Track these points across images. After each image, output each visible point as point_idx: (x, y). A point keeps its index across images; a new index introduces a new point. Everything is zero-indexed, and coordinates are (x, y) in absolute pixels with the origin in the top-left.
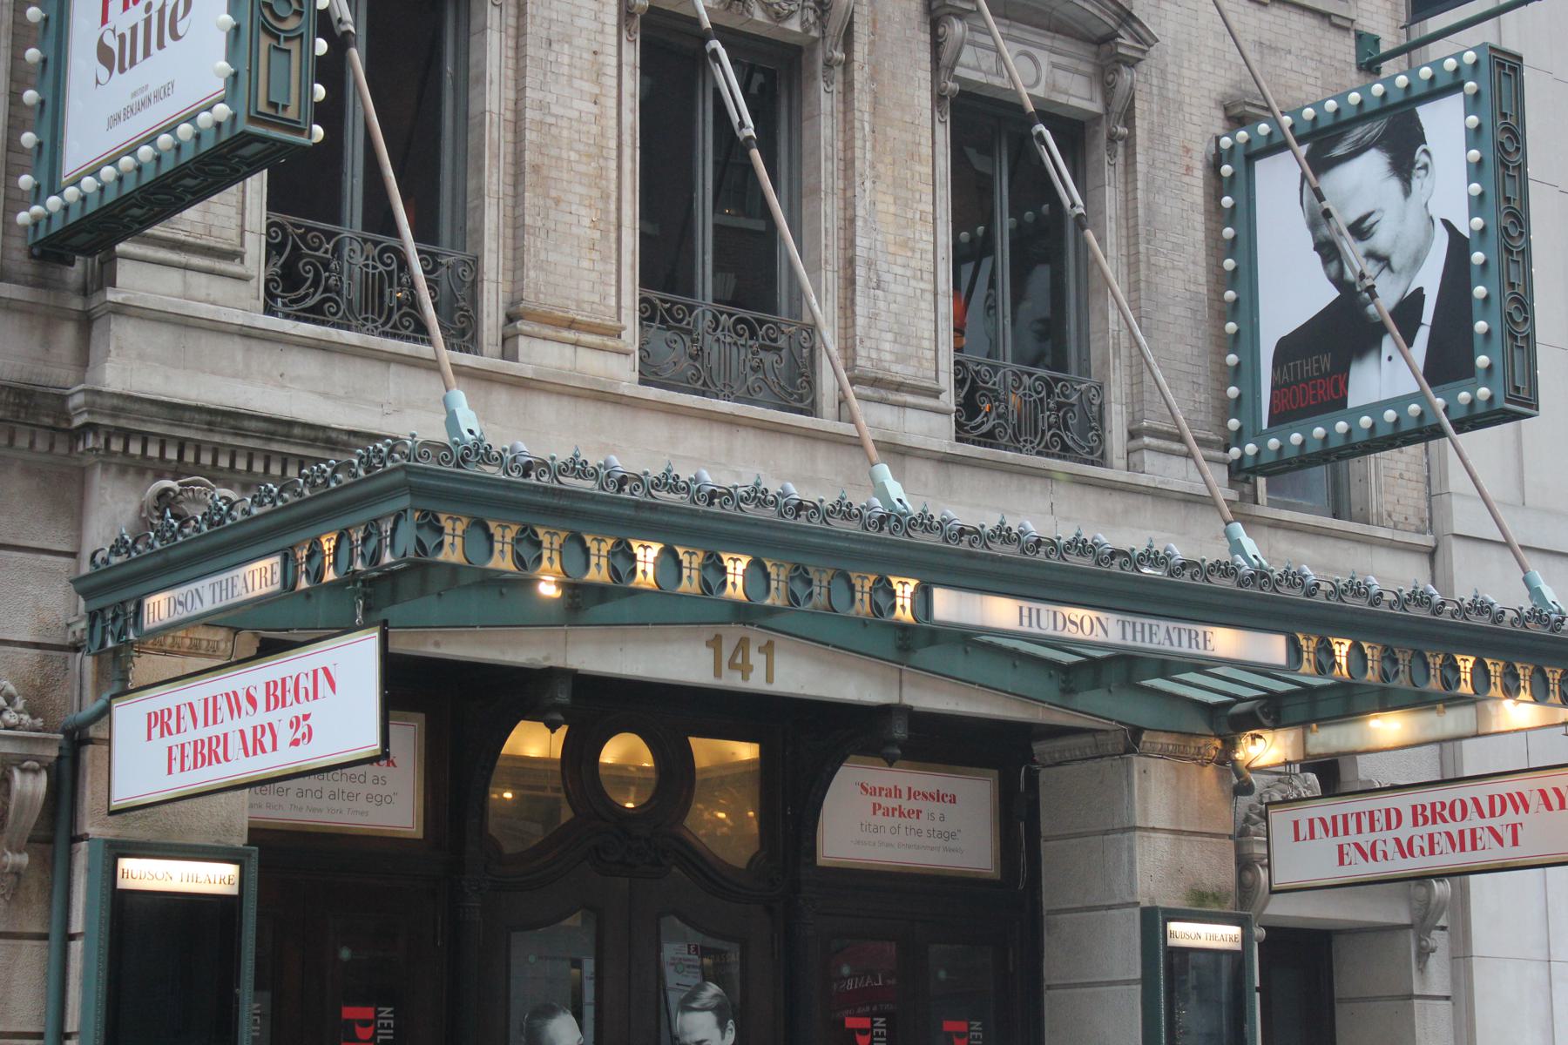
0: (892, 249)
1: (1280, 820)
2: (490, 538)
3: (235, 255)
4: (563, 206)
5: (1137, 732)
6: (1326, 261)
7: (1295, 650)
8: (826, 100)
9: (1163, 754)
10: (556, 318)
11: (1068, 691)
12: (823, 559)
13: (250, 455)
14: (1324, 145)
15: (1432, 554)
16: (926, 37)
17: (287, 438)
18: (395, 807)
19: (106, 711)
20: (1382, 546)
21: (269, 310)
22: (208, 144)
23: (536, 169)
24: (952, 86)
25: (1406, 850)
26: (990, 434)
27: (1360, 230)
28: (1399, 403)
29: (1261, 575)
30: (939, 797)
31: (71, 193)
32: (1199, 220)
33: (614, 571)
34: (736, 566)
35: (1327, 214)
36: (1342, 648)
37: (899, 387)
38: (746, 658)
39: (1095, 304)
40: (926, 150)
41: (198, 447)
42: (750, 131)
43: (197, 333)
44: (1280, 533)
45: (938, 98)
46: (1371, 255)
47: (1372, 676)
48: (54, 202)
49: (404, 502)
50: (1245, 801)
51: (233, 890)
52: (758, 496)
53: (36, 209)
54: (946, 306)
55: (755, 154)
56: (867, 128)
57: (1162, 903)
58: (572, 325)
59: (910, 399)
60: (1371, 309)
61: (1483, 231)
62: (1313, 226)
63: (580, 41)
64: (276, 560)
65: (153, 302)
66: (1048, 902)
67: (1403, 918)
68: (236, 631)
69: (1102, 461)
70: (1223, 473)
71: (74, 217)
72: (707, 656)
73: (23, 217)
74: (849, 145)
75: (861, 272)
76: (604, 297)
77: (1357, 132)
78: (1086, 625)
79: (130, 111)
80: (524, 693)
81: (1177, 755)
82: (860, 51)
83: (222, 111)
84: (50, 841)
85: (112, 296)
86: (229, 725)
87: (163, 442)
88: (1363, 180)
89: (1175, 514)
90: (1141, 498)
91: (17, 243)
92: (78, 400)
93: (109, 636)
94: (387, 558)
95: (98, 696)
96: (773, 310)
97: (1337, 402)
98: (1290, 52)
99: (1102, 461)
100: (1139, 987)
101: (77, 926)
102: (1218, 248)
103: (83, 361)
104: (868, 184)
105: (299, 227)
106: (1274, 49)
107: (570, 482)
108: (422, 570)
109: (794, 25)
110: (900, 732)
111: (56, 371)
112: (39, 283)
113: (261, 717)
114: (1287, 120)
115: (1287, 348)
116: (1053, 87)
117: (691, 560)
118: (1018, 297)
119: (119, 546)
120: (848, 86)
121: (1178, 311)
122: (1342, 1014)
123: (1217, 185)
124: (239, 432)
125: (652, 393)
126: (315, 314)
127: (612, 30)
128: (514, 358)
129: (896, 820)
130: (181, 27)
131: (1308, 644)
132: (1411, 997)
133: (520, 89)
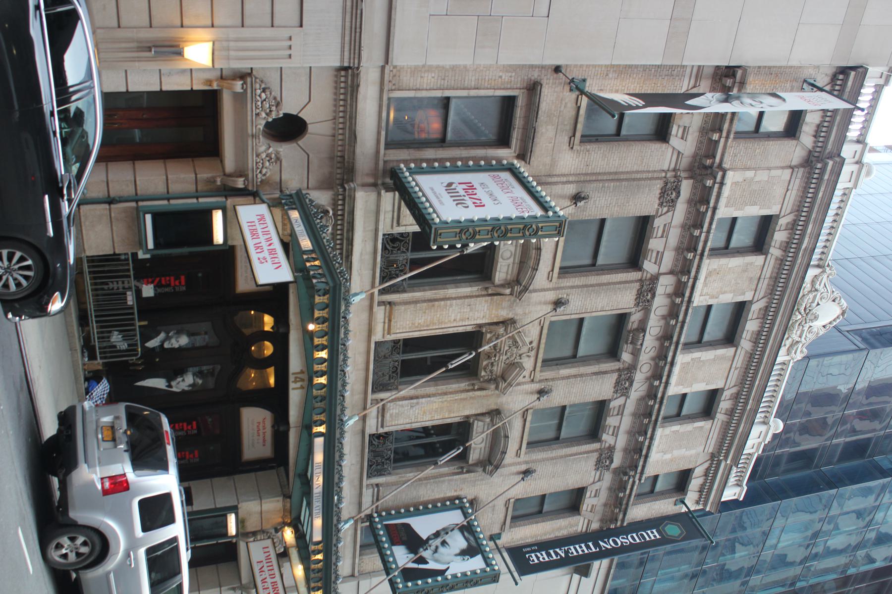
1: (268, 542)
2: (323, 309)
3: (398, 224)
5: (290, 497)
6: (434, 534)
7: (318, 543)
8: (463, 385)
9: (284, 506)
11: (300, 476)
12: (329, 405)
13: (342, 235)
14: (467, 529)
15: (353, 576)
16: (484, 411)
17: (348, 245)
18: (243, 285)
19: (263, 202)
21: (384, 235)
22: (427, 217)
23: (433, 306)
24: (471, 420)
25: (264, 581)
27: (444, 543)
28: (395, 561)
29: (339, 531)
30: (264, 441)
31: (410, 179)
32: (442, 496)
33: (318, 346)
34: (323, 380)
35: (447, 533)
36: (320, 557)
37: (383, 416)
39: (414, 469)
40: (452, 415)
41: (342, 220)
42: (450, 367)
43: (374, 217)
45: (468, 417)
46: (437, 547)
47: (313, 566)
48: (407, 174)
49: (331, 284)
50: (273, 531)
51: (215, 243)
52: (344, 385)
53: (405, 169)
54: (408, 427)
55: (444, 369)
57: (240, 511)
58: (390, 321)
59: (380, 420)
60: (421, 550)
61: (447, 579)
62: (444, 529)
63: (471, 314)
64: (311, 248)
65: (383, 203)
66: (237, 477)
67: (244, 581)
68: (291, 235)
69: (368, 477)
70: (368, 512)
71: (404, 180)
72: (298, 370)
73: (402, 166)
74: (451, 393)
75: (415, 401)
77: (472, 538)
78: (318, 482)
79: (435, 193)
80: (282, 319)
81: (284, 510)
82: (478, 393)
83: (437, 220)
84: (225, 190)
85: (383, 192)
86: (262, 239)
87: (343, 210)
88: (458, 542)
89: (355, 500)
91: (395, 164)
92: (352, 185)
93: (285, 201)
94: (314, 281)
95: (269, 199)
96: (401, 377)
97: (394, 542)
99: (368, 477)
100: (213, 507)
101: (201, 200)
102: (434, 502)
103: (364, 185)
106: (493, 510)
107: (342, 331)
108: (312, 290)
109: (483, 373)
110: (282, 429)
111: (360, 178)
112: (384, 171)
113: (266, 248)
114: (473, 517)
115: (407, 526)
116: (475, 449)
117: (323, 367)
118: (415, 446)
119: (311, 201)
120: (468, 391)
121: (415, 493)
122: (213, 567)
123: (452, 499)
124: (348, 231)
125: (373, 346)
126: (384, 248)
127: (475, 322)
128: (379, 305)
129: (256, 429)
130: (459, 206)
131: (320, 547)
132: (221, 587)
133: (455, 298)
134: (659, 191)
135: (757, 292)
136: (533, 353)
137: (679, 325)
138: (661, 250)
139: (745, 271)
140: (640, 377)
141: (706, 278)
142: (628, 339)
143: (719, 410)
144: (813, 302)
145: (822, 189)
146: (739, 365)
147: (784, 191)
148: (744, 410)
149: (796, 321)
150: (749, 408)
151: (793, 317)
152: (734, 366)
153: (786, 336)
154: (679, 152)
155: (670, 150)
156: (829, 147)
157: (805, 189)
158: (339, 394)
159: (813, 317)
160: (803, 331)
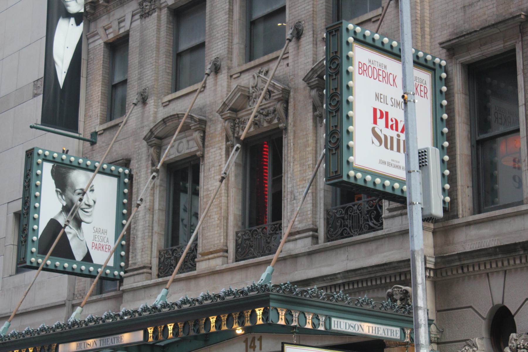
0: (298, 183)
4: (211, 217)
10: (207, 253)
20: (463, 226)
26: (342, 234)
38: (254, 344)
44: (472, 227)
56: (292, 144)
58: (211, 253)
76: (220, 240)
85: (121, 289)
90: (383, 240)
104: (292, 164)
105: (277, 224)
106: (471, 5)
127: (224, 156)
134: (147, 19)
136: (265, 69)
154: (133, 16)
155: (134, 24)
158: (73, 328)
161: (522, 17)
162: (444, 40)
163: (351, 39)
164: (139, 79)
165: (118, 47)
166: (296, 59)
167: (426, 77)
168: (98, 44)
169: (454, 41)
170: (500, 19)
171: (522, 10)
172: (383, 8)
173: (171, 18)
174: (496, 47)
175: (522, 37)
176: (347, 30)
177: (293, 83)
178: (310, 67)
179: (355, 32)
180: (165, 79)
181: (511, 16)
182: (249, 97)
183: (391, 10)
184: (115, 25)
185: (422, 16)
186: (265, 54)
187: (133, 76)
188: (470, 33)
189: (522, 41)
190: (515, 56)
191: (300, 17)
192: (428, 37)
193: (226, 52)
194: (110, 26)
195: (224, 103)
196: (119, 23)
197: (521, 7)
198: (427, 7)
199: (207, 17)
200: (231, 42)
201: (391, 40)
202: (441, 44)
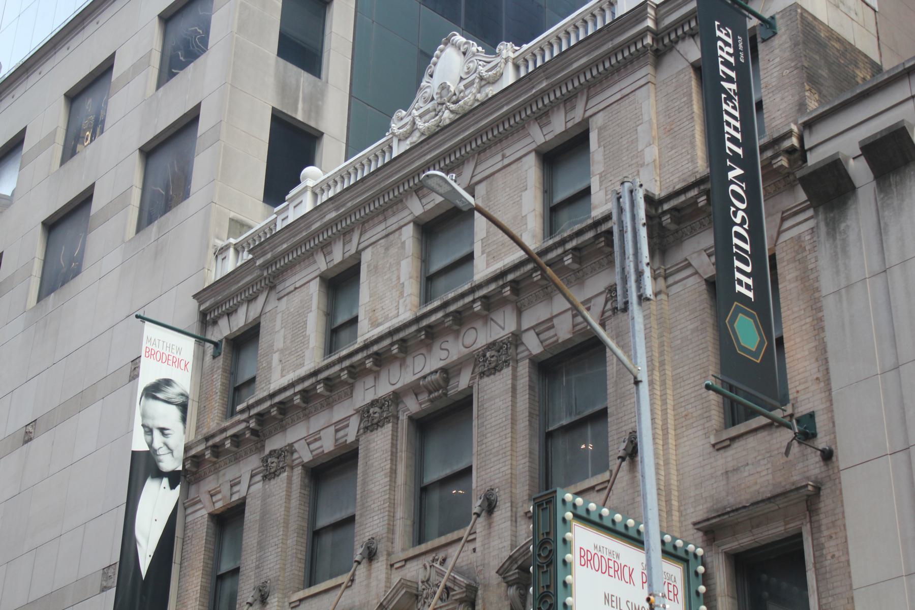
98: (748, 464)
106: (736, 470)
134: (273, 482)
135: (402, 223)
136: (441, 555)
137: (396, 338)
138: (332, 429)
139: (376, 267)
140: (480, 337)
141: (379, 325)
142: (440, 397)
143: (570, 125)
144: (427, 112)
145: (280, 249)
146: (499, 157)
147: (297, 293)
148: (552, 88)
149: (452, 112)
150: (544, 84)
151: (448, 122)
152: (499, 166)
153: (477, 104)
154: (252, 476)
155: (253, 488)
156: (255, 275)
157: (290, 267)
159: (444, 92)
160: (466, 87)
161: (810, 488)
162: (699, 518)
163: (569, 515)
164: (258, 567)
165: (228, 520)
166: (486, 541)
167: (675, 571)
168: (201, 516)
169: (714, 521)
170: (779, 490)
171: (808, 478)
172: (611, 471)
173: (307, 481)
174: (774, 531)
175: (810, 517)
176: (564, 501)
177: (482, 577)
178: (506, 554)
179: (574, 505)
180: (296, 569)
181: (793, 487)
182: (417, 596)
183: (624, 475)
184: (226, 489)
185: (668, 485)
186: (441, 534)
187: (248, 562)
188: (737, 510)
189: (811, 522)
190: (801, 543)
191: (492, 483)
192: (676, 514)
193: (385, 531)
194: (218, 490)
195: (381, 604)
196: (232, 486)
197: (807, 474)
198: (673, 472)
199: (359, 480)
200: (392, 517)
201: (625, 518)
202: (695, 524)
